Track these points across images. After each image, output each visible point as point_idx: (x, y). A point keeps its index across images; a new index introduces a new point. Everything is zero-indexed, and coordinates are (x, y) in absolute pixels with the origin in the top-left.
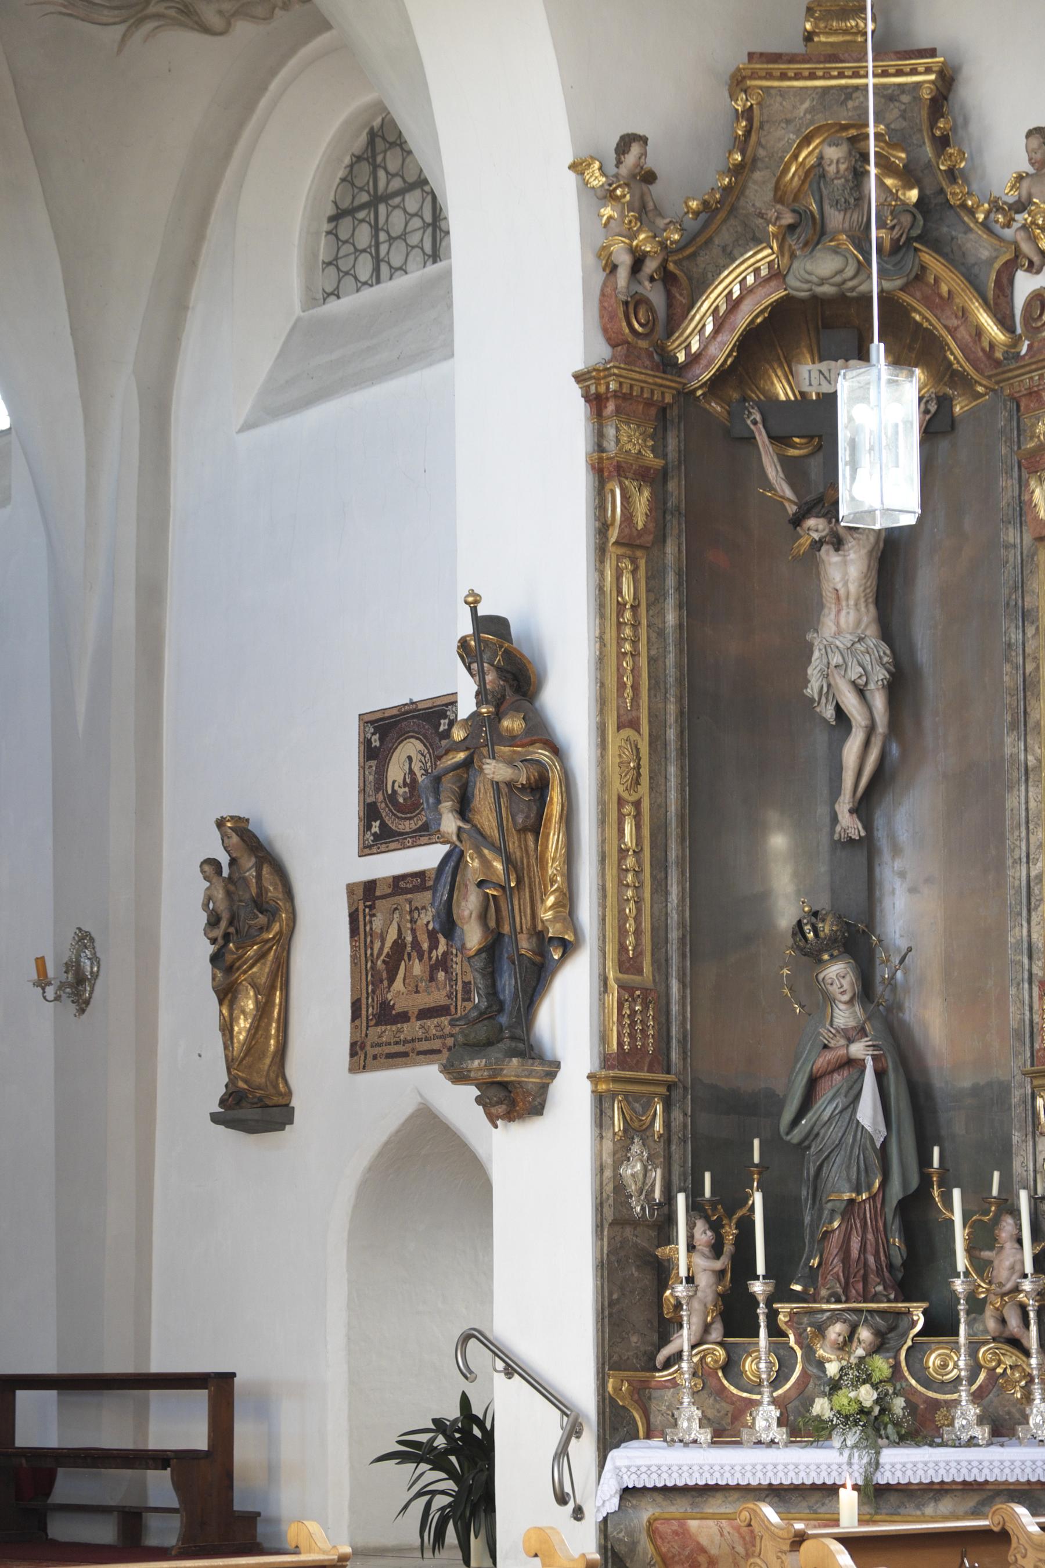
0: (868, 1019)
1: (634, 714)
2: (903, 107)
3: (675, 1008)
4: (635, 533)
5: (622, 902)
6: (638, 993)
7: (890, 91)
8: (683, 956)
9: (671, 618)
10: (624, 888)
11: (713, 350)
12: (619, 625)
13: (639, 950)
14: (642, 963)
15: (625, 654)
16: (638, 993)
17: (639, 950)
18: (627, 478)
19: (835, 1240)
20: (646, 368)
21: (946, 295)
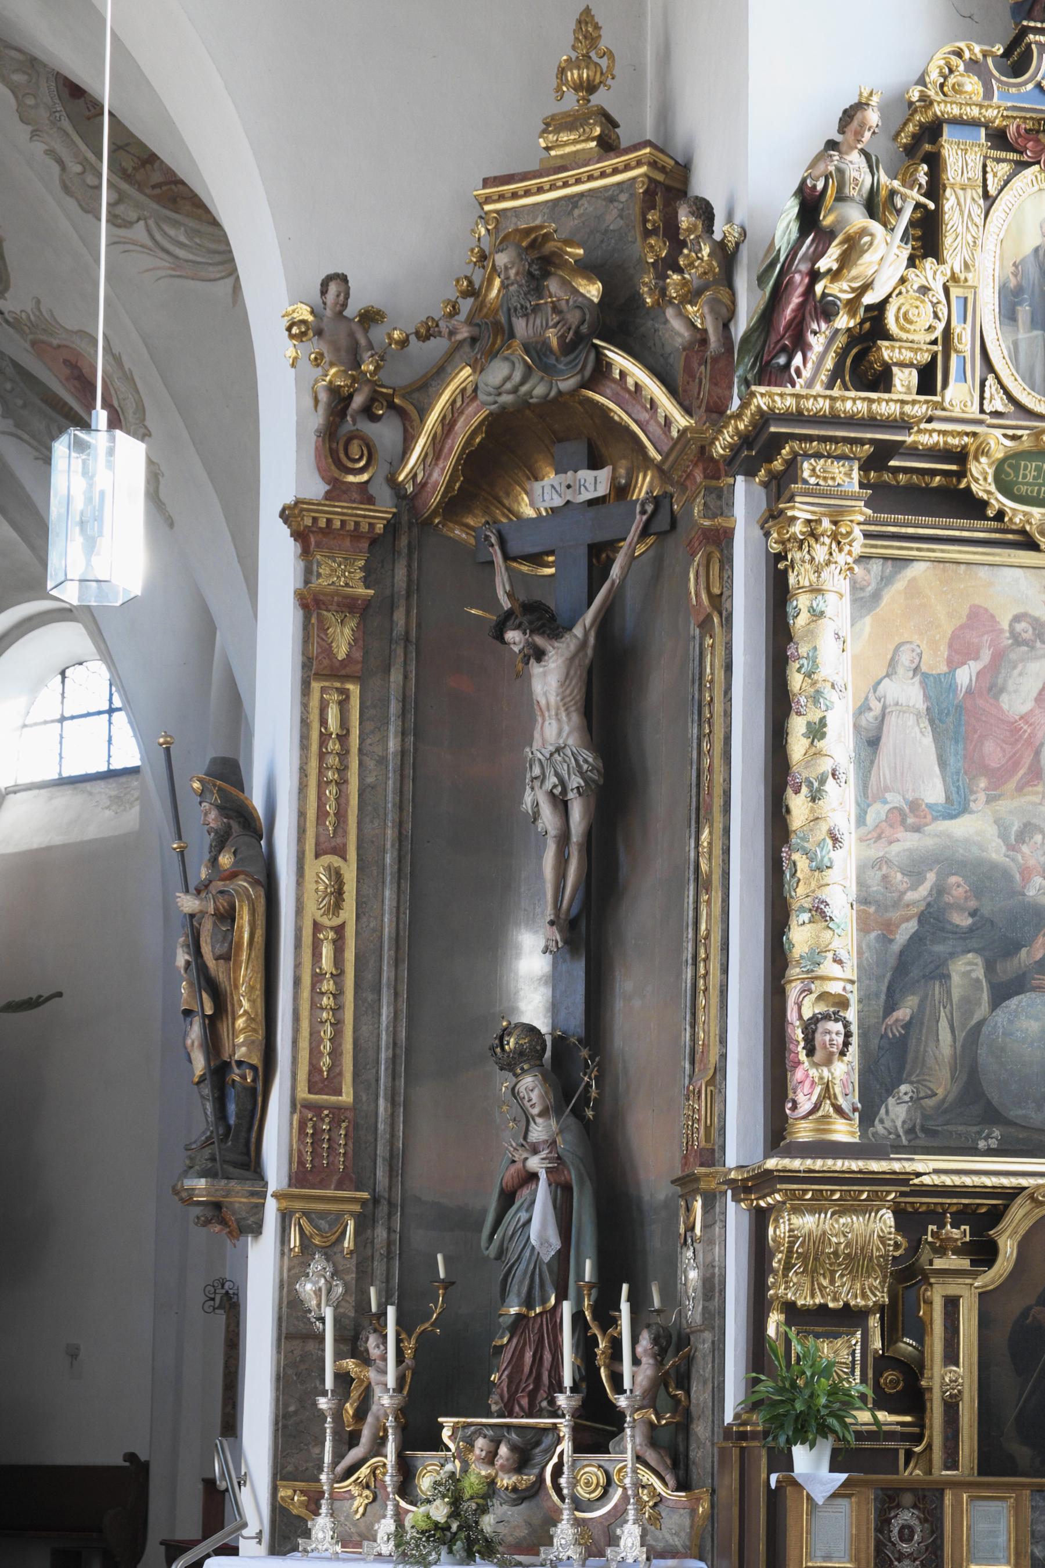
0: (561, 1131)
2: (621, 206)
3: (381, 1127)
4: (337, 664)
5: (316, 1025)
6: (326, 1112)
7: (610, 193)
8: (394, 1076)
9: (393, 745)
10: (319, 1011)
11: (435, 475)
13: (337, 1070)
14: (340, 1083)
16: (326, 1112)
17: (337, 1070)
18: (328, 611)
19: (507, 1356)
20: (354, 502)
21: (632, 389)
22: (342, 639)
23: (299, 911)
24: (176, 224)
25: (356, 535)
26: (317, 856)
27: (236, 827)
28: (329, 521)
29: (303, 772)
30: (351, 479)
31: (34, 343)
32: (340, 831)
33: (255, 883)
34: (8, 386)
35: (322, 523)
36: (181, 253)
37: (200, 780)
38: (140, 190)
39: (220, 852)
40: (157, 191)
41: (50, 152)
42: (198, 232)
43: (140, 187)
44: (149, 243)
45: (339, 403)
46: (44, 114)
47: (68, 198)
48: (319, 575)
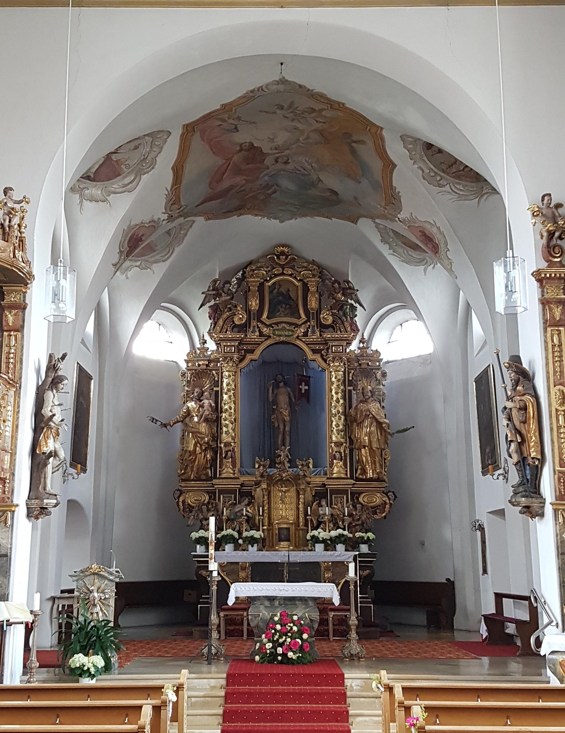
1: (562, 381)
12: (553, 352)
15: (556, 361)
22: (558, 312)
23: (550, 405)
24: (459, 184)
25: (560, 278)
26: (555, 386)
27: (521, 378)
28: (550, 275)
29: (547, 358)
30: (556, 260)
31: (409, 227)
32: (562, 377)
33: (532, 396)
34: (391, 240)
35: (548, 275)
36: (461, 193)
37: (507, 363)
38: (448, 175)
39: (517, 386)
40: (454, 174)
41: (420, 168)
42: (466, 186)
43: (448, 174)
44: (451, 191)
45: (551, 235)
46: (418, 156)
47: (424, 181)
48: (547, 293)
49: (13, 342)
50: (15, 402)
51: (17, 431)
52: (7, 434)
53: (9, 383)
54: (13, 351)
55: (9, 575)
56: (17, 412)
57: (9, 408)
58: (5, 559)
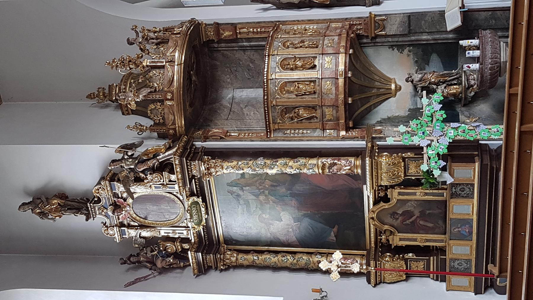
49: (245, 30)
50: (291, 24)
51: (313, 20)
52: (315, 27)
53: (276, 29)
54: (251, 30)
55: (425, 12)
56: (298, 22)
57: (295, 28)
58: (412, 17)
